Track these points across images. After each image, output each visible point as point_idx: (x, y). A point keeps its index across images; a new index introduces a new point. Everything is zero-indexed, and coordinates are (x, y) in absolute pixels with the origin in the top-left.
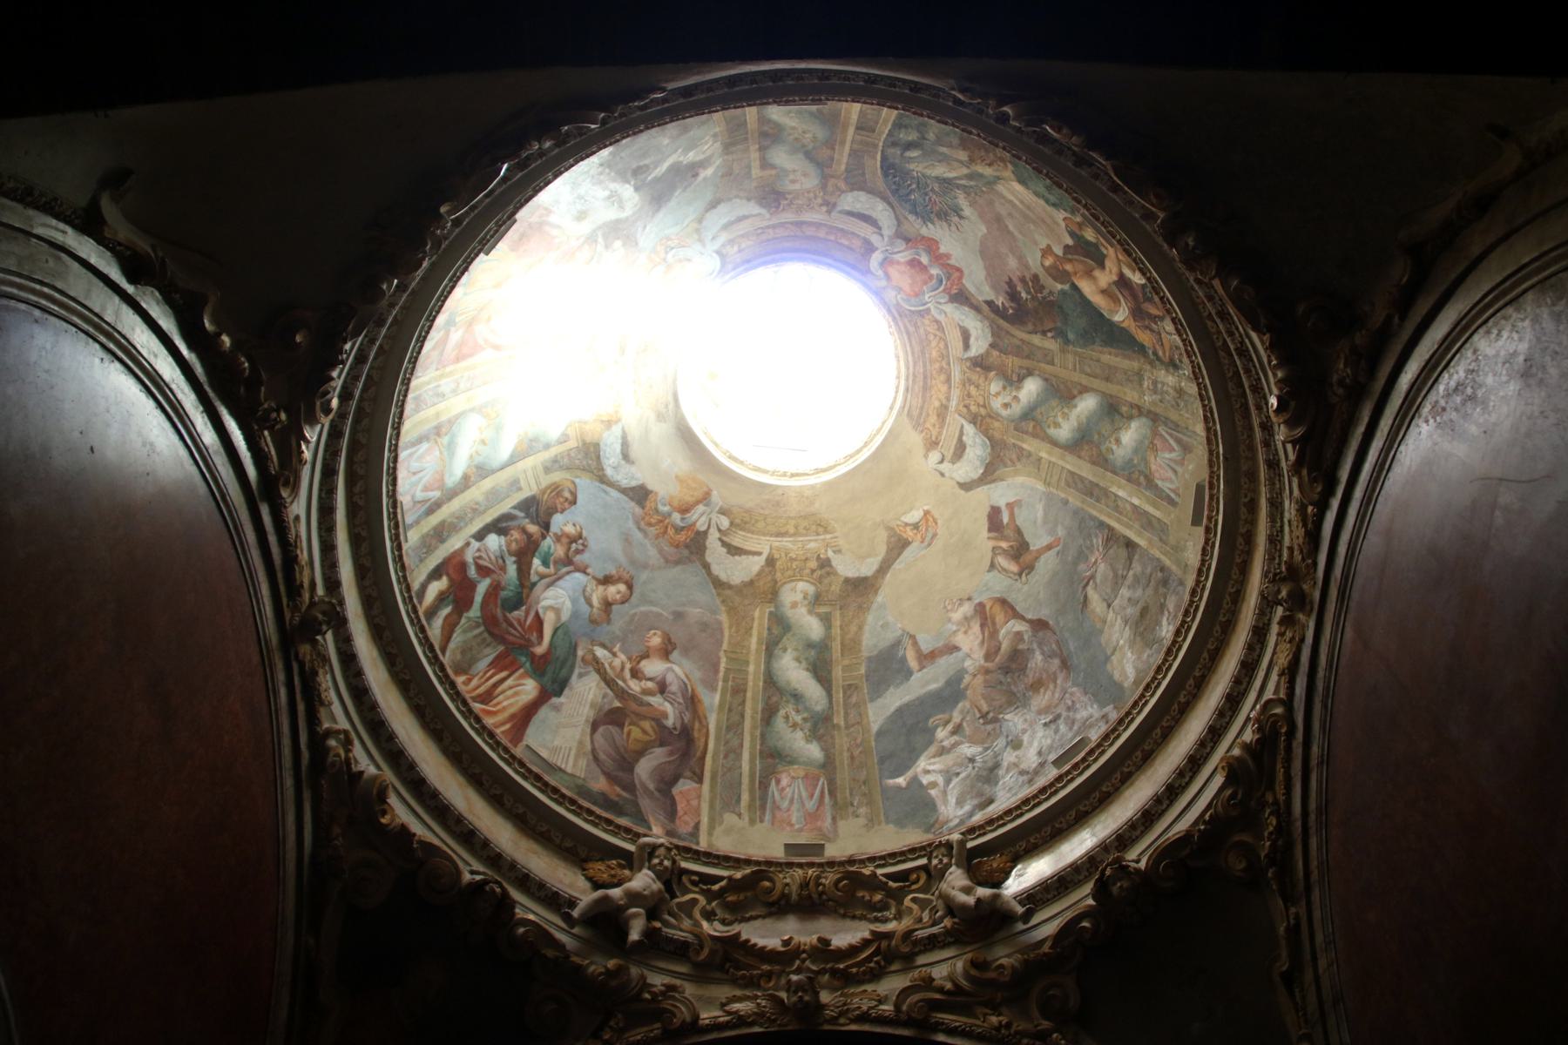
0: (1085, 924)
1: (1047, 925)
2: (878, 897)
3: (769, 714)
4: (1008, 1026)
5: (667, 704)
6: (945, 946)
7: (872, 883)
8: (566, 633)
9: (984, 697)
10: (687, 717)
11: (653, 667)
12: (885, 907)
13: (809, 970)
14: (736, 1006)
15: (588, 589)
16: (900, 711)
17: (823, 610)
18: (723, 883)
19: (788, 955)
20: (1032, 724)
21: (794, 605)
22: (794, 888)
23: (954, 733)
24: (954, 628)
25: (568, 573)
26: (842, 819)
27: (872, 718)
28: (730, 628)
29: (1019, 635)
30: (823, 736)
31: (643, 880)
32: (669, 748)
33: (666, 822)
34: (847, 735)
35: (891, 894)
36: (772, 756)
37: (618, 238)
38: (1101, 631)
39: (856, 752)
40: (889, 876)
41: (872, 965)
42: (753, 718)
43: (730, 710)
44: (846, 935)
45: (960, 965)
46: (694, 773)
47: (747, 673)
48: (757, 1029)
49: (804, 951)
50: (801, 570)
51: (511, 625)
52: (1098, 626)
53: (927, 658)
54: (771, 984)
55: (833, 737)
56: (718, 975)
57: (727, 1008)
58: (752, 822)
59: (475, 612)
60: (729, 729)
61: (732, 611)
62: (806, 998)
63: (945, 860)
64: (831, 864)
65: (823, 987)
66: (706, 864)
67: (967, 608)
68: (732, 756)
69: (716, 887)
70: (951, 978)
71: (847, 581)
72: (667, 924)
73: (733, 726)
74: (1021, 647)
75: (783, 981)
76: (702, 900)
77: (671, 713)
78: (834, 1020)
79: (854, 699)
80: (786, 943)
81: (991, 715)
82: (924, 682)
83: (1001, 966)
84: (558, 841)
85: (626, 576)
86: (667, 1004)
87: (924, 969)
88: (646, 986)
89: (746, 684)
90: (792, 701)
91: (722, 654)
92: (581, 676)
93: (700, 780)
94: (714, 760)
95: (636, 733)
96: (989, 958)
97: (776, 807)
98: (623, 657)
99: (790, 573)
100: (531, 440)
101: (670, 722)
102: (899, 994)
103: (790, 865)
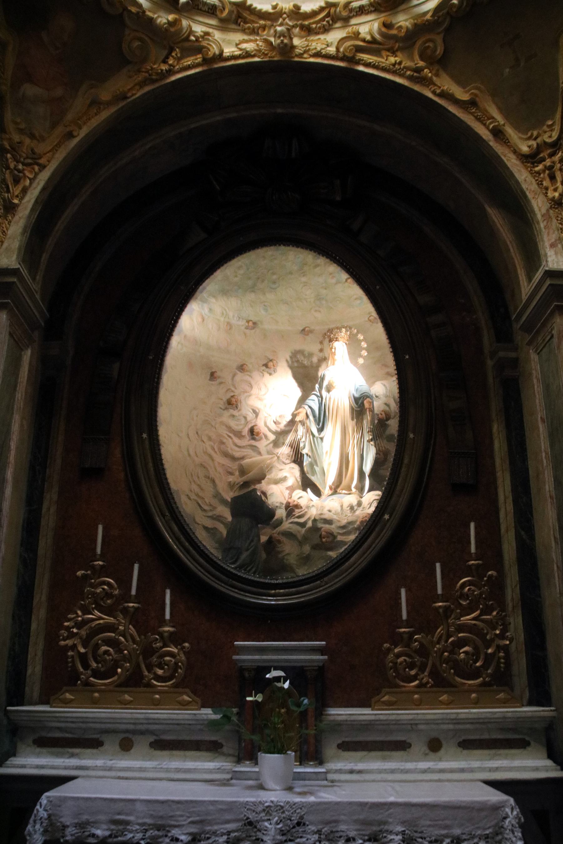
4: (400, 63)
6: (368, 13)
13: (287, 24)
14: (244, 46)
41: (325, 23)
45: (376, 25)
48: (256, 59)
49: (285, 13)
54: (265, 33)
56: (234, 26)
57: (239, 46)
62: (286, 41)
65: (295, 36)
75: (272, 31)
78: (300, 55)
80: (274, 7)
83: (400, 27)
86: (204, 43)
87: (355, 27)
88: (191, 32)
96: (394, 22)
102: (338, 43)
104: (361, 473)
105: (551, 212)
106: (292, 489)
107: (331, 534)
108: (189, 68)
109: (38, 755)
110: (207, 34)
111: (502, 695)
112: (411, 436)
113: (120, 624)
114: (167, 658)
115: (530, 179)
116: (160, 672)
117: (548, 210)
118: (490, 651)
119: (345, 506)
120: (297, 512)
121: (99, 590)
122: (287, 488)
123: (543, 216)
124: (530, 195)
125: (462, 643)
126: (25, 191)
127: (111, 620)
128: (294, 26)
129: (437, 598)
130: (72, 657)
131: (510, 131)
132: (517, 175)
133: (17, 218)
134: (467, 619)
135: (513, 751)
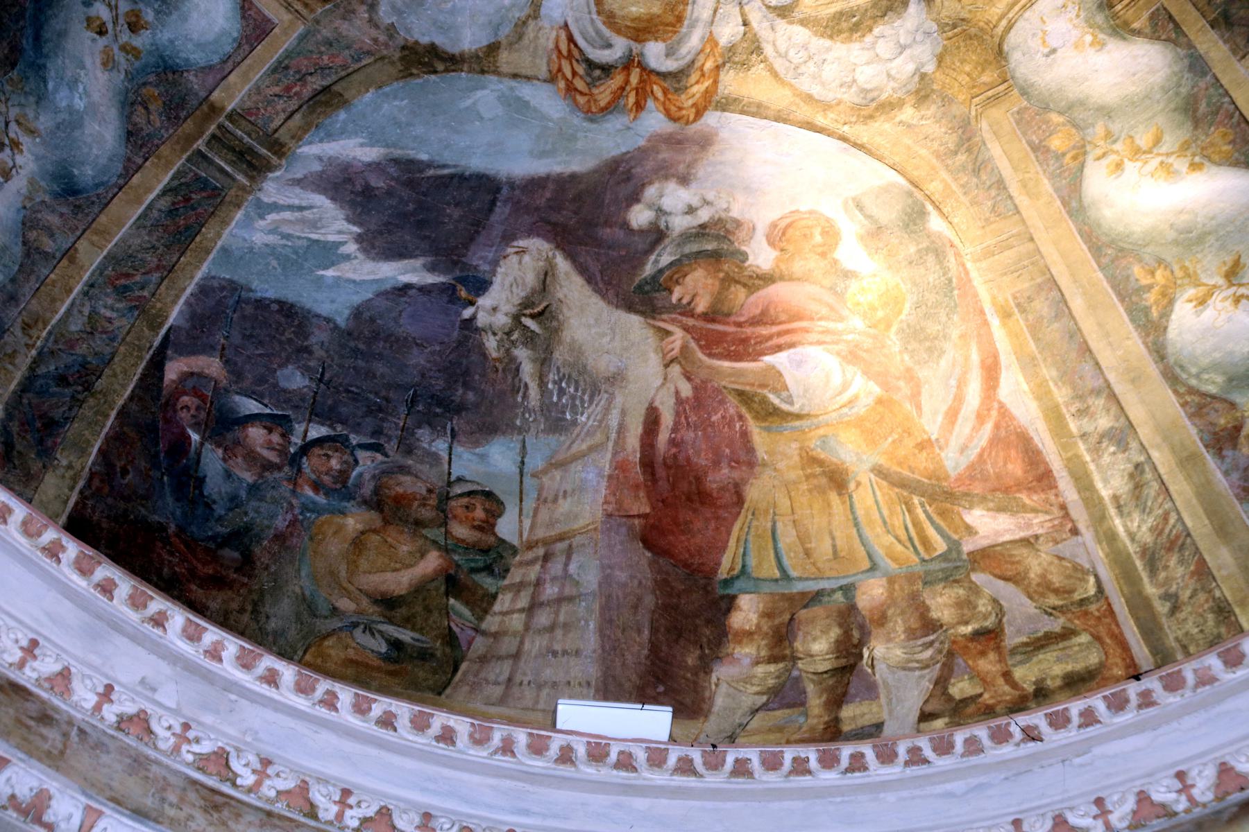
37: (625, 225)
100: (1196, 123)
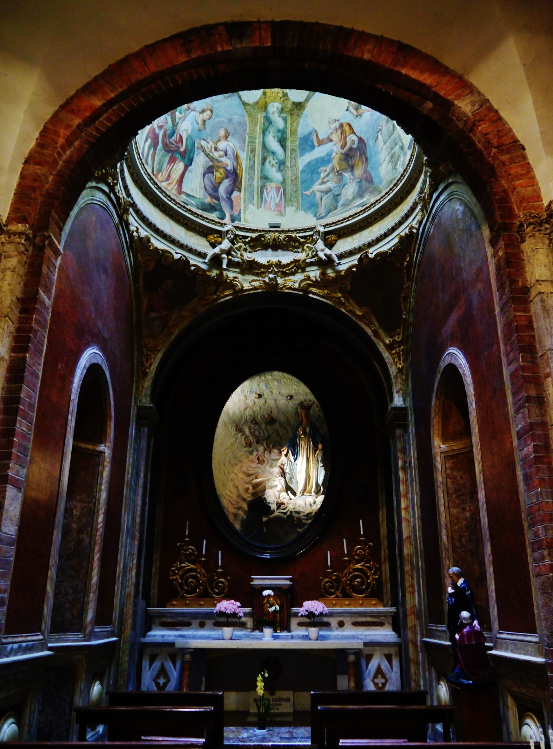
0: (354, 269)
1: (344, 265)
2: (297, 244)
3: (264, 160)
4: (330, 294)
5: (228, 160)
7: (295, 240)
8: (191, 138)
9: (339, 164)
10: (235, 164)
11: (222, 145)
12: (298, 248)
14: (253, 283)
15: (197, 117)
16: (309, 163)
17: (284, 115)
18: (249, 239)
19: (269, 266)
20: (353, 180)
21: (273, 113)
22: (271, 241)
23: (327, 176)
24: (332, 131)
25: (189, 113)
26: (288, 206)
27: (300, 165)
28: (249, 123)
29: (353, 142)
30: (282, 170)
31: (226, 244)
32: (230, 179)
33: (230, 210)
34: (291, 170)
35: (301, 243)
36: (265, 178)
38: (380, 153)
39: (293, 178)
40: (301, 237)
42: (258, 163)
43: (250, 159)
44: (286, 258)
46: (239, 188)
47: (255, 143)
48: (260, 291)
50: (276, 97)
51: (172, 144)
52: (380, 149)
53: (321, 143)
55: (286, 171)
58: (258, 208)
59: (160, 146)
60: (249, 168)
61: (250, 115)
63: (318, 237)
64: (283, 231)
66: (244, 232)
67: (337, 124)
68: (251, 180)
69: (247, 240)
70: (315, 277)
71: (294, 103)
72: (233, 256)
73: (252, 167)
74: (354, 146)
76: (244, 247)
77: (229, 163)
78: (281, 289)
79: (293, 156)
80: (268, 262)
81: (340, 172)
82: (319, 152)
83: (330, 276)
84: (198, 229)
85: (210, 107)
88: (228, 277)
89: (255, 148)
90: (272, 155)
91: (246, 135)
92: (197, 154)
93: (240, 191)
94: (245, 182)
95: (218, 175)
97: (266, 201)
98: (211, 143)
99: (272, 98)
101: (229, 168)
103: (270, 231)
104: (317, 484)
105: (398, 374)
106: (280, 492)
107: (299, 519)
108: (227, 296)
109: (162, 630)
110: (235, 278)
111: (374, 602)
112: (337, 474)
113: (198, 568)
114: (220, 584)
115: (390, 357)
116: (217, 591)
117: (397, 374)
118: (369, 581)
119: (307, 504)
120: (282, 507)
121: (188, 552)
122: (278, 491)
123: (394, 376)
124: (389, 365)
125: (357, 577)
126: (151, 364)
127: (194, 566)
128: (279, 272)
129: (345, 556)
130: (176, 584)
131: (381, 331)
132: (383, 355)
133: (148, 378)
134: (358, 566)
135: (377, 627)
